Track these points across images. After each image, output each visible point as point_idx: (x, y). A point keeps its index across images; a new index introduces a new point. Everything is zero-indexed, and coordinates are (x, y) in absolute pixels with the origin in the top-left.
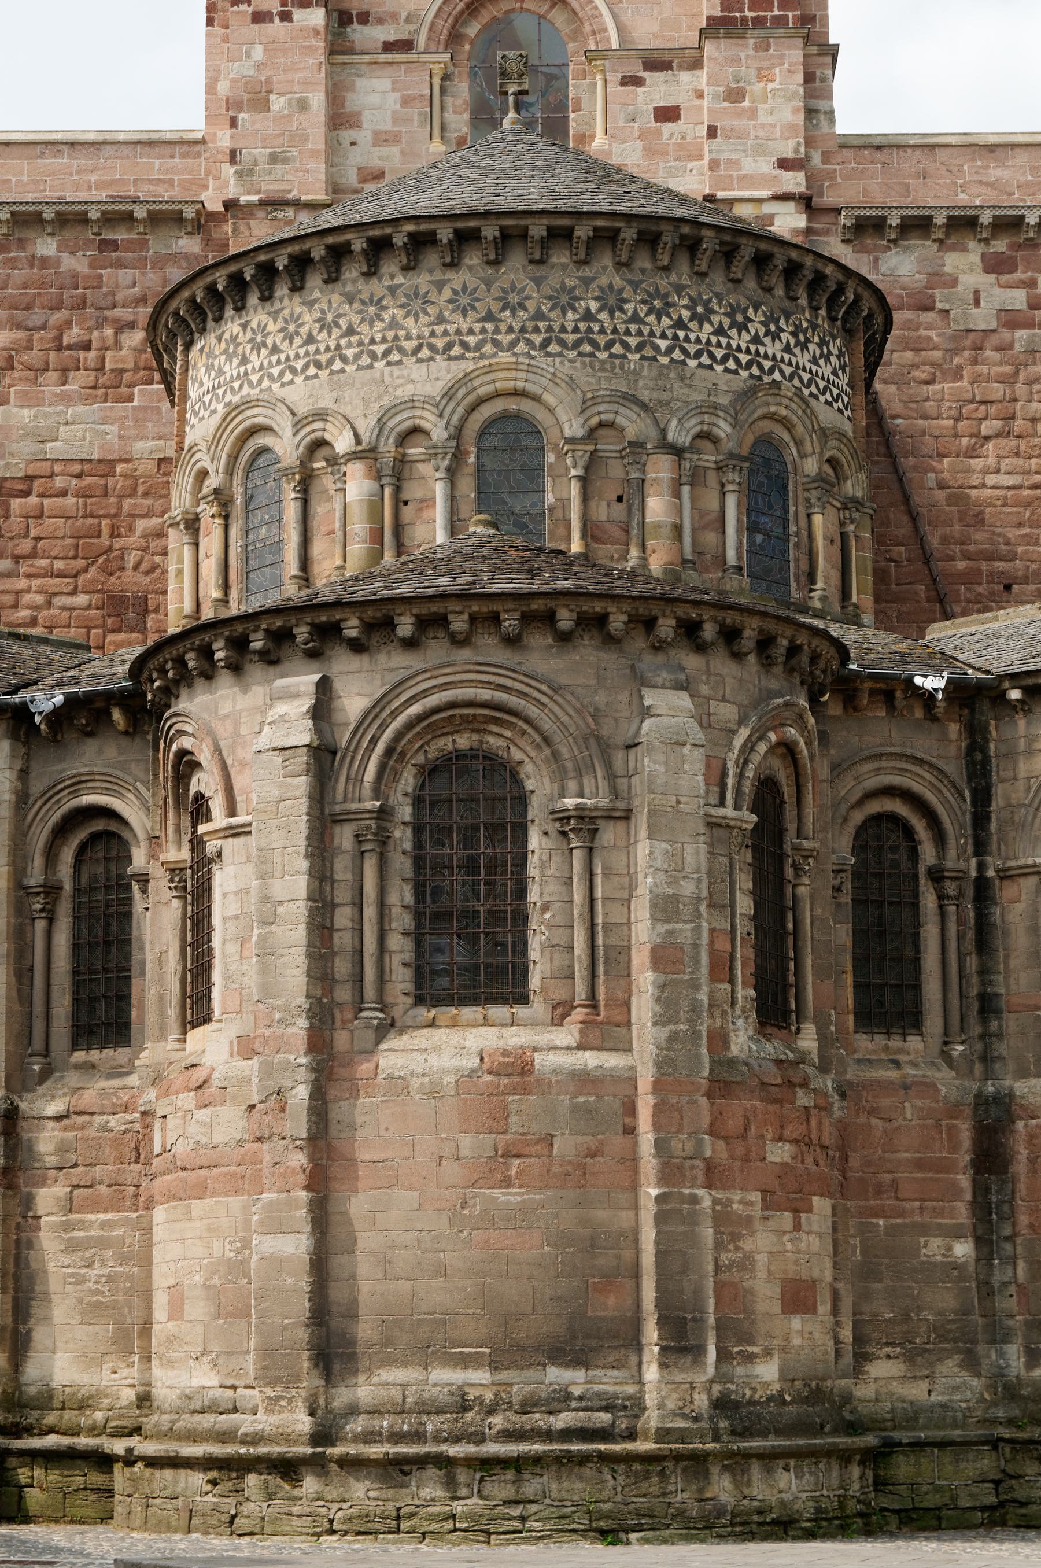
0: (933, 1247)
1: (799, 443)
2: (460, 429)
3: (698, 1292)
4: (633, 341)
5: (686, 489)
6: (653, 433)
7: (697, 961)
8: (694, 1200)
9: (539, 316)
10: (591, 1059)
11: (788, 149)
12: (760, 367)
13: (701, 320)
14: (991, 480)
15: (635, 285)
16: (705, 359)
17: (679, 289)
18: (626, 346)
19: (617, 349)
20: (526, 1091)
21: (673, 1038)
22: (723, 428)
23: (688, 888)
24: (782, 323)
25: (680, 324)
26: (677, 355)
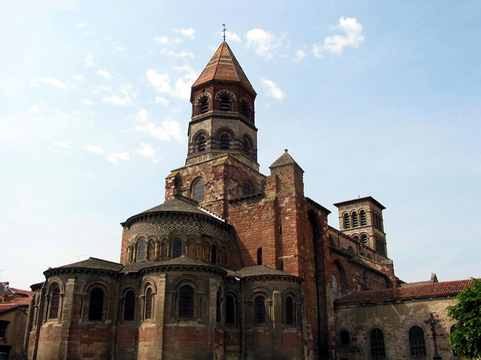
0: (128, 350)
1: (183, 238)
2: (137, 242)
3: (64, 355)
4: (155, 228)
5: (161, 247)
6: (156, 240)
7: (69, 312)
8: (65, 342)
9: (145, 226)
10: (58, 325)
11: (221, 193)
12: (175, 228)
13: (165, 224)
14: (247, 235)
15: (156, 221)
16: (166, 229)
17: (162, 220)
18: (154, 229)
19: (153, 229)
20: (51, 329)
21: (65, 322)
22: (167, 238)
23: (69, 303)
24: (181, 221)
25: (162, 225)
26: (161, 229)
